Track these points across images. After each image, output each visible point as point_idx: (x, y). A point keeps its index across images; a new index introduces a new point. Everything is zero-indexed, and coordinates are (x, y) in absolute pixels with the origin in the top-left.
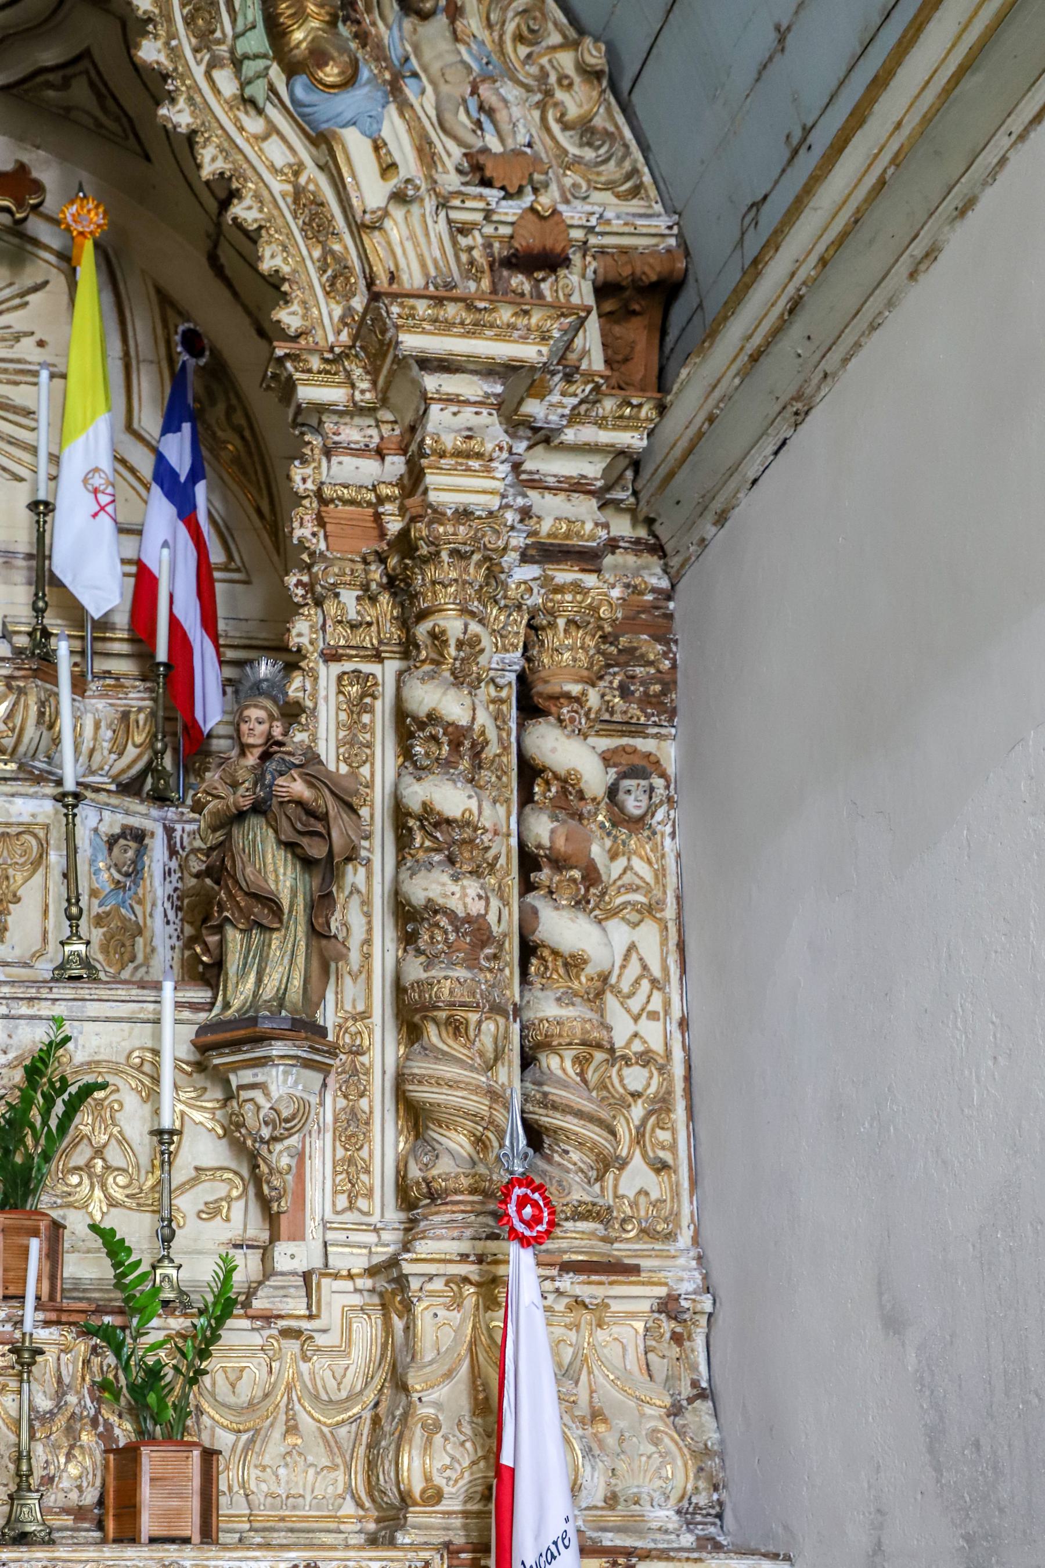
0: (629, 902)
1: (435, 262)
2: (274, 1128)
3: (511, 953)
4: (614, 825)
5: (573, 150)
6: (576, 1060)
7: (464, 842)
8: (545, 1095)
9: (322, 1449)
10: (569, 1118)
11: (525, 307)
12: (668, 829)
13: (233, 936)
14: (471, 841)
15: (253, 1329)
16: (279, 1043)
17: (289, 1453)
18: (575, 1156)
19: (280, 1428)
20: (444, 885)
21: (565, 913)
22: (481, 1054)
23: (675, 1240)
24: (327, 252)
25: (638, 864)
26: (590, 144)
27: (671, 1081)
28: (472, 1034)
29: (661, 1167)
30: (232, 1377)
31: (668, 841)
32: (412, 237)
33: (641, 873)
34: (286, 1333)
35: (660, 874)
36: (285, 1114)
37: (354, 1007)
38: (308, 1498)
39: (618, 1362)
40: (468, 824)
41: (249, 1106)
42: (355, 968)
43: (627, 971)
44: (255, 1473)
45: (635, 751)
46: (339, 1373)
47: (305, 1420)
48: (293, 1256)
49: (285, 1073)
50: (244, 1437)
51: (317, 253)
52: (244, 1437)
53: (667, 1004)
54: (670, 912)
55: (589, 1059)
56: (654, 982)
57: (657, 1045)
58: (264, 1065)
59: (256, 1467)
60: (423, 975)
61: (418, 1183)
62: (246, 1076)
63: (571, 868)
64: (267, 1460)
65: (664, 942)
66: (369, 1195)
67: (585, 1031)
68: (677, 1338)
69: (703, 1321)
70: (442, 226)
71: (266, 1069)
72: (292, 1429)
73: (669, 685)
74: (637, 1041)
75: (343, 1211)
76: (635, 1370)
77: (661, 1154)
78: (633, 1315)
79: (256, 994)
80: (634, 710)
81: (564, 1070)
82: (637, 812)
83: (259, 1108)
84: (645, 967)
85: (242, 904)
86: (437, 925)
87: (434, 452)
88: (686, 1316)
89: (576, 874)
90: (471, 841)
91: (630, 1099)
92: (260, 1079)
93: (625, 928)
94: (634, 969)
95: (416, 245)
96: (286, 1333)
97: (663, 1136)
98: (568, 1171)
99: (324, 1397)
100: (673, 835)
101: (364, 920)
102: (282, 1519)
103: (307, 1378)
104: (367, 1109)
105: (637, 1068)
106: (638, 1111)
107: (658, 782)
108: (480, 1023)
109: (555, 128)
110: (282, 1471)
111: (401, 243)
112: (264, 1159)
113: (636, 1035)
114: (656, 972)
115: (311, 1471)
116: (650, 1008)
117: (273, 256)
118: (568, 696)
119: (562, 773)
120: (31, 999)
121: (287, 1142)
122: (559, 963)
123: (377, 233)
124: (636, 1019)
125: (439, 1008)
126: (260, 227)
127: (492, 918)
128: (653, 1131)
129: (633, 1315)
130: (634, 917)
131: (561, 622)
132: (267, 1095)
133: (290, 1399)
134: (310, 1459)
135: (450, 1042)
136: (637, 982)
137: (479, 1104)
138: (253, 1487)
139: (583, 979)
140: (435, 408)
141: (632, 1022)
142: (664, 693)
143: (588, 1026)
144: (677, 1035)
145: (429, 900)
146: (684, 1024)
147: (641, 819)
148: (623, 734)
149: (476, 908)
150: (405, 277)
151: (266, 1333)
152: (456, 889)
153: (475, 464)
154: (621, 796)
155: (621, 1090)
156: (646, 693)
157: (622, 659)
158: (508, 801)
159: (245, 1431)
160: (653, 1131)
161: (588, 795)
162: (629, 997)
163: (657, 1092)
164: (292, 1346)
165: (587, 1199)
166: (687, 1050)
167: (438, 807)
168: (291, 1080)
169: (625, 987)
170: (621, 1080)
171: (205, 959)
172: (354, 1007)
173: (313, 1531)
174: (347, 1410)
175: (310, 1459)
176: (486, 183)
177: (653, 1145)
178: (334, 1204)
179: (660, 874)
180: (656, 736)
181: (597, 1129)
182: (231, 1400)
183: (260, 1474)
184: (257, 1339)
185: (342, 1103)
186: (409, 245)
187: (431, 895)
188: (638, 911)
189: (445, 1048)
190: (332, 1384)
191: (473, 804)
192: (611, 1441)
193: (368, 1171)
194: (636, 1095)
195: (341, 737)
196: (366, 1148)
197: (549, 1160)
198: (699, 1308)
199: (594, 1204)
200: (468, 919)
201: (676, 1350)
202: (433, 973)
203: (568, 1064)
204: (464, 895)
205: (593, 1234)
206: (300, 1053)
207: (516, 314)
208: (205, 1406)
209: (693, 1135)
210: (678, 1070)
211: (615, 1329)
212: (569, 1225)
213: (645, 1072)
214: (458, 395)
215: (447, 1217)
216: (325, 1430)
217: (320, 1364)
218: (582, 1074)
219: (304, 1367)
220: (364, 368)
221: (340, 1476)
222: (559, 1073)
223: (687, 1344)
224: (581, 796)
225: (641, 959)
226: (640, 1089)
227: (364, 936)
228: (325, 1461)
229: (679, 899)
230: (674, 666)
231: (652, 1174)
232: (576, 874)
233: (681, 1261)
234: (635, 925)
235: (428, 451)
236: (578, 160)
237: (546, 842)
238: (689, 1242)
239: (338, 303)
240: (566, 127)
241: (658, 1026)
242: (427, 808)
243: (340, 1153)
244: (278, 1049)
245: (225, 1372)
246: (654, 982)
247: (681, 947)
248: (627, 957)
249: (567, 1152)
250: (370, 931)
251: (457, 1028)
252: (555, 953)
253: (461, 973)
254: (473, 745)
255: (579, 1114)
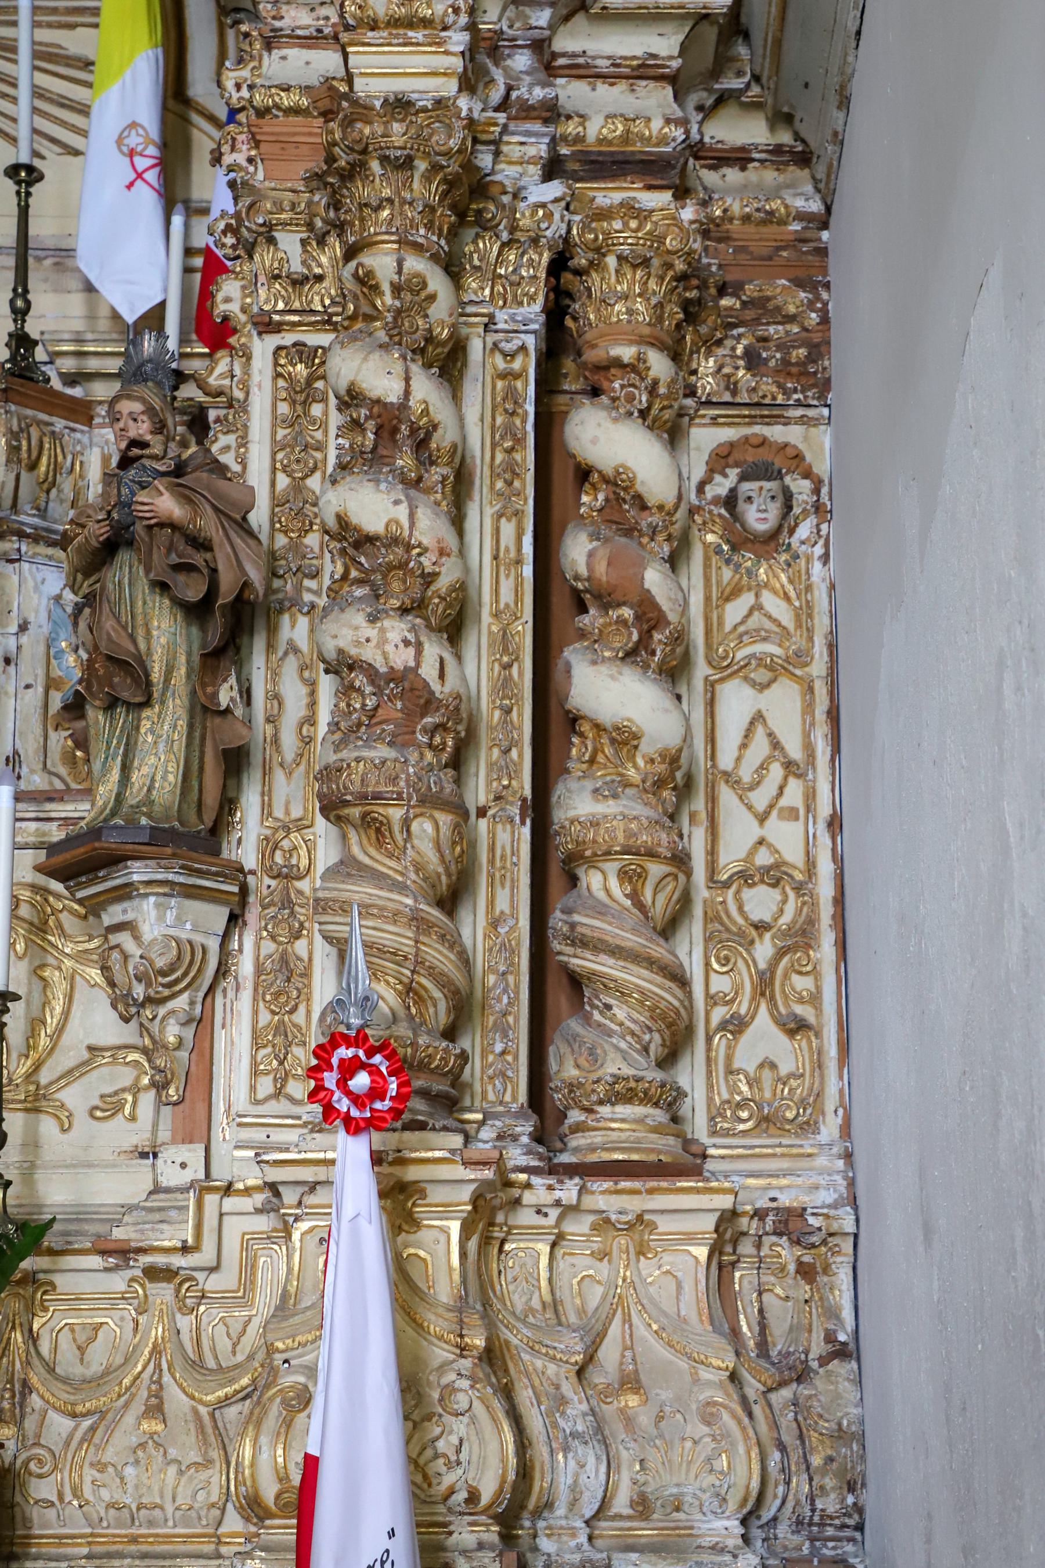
0: (753, 656)
2: (149, 985)
3: (520, 728)
4: (734, 548)
6: (623, 875)
7: (391, 567)
8: (573, 926)
10: (603, 958)
12: (819, 550)
14: (403, 565)
15: (107, 1270)
17: (142, 1445)
18: (620, 1012)
19: (138, 1407)
20: (357, 628)
21: (604, 669)
22: (418, 868)
23: (816, 1131)
25: (771, 603)
27: (814, 905)
28: (399, 838)
29: (796, 1027)
30: (82, 1338)
31: (817, 567)
33: (775, 614)
34: (152, 1273)
35: (804, 614)
36: (160, 963)
37: (287, 812)
38: (170, 1509)
39: (669, 1307)
40: (395, 541)
42: (289, 755)
43: (749, 753)
44: (89, 1474)
45: (764, 442)
46: (236, 1328)
47: (176, 1399)
48: (183, 1166)
49: (157, 905)
50: (87, 1423)
52: (87, 1423)
53: (810, 796)
54: (818, 667)
55: (642, 875)
56: (790, 767)
57: (793, 854)
58: (129, 897)
59: (92, 1465)
63: (619, 605)
64: (109, 1455)
65: (808, 708)
67: (630, 834)
68: (806, 1272)
69: (847, 1246)
71: (136, 902)
72: (156, 1409)
73: (819, 349)
74: (763, 850)
75: (266, 1099)
76: (693, 1317)
77: (799, 1009)
78: (690, 1238)
79: (119, 798)
80: (768, 386)
81: (607, 891)
82: (761, 527)
83: (126, 957)
84: (776, 745)
88: (815, 1239)
89: (627, 613)
90: (403, 565)
91: (754, 933)
92: (129, 916)
93: (748, 691)
94: (760, 747)
96: (152, 1273)
97: (802, 983)
98: (610, 1033)
99: (211, 1364)
100: (825, 558)
101: (304, 690)
102: (134, 1540)
103: (186, 1338)
104: (305, 955)
105: (762, 889)
106: (764, 950)
107: (801, 488)
108: (406, 823)
110: (129, 1471)
113: (761, 842)
114: (795, 751)
115: (172, 1470)
116: (783, 802)
118: (617, 363)
119: (609, 472)
121: (171, 1005)
122: (605, 740)
124: (762, 818)
125: (346, 804)
127: (429, 671)
128: (786, 976)
129: (690, 1238)
130: (761, 675)
131: (611, 261)
132: (137, 938)
133: (158, 1367)
134: (173, 1453)
135: (372, 851)
136: (763, 767)
138: (87, 1492)
139: (640, 762)
141: (755, 823)
142: (811, 359)
144: (824, 840)
146: (835, 824)
147: (773, 536)
148: (752, 420)
149: (402, 658)
151: (129, 1274)
152: (372, 632)
154: (741, 505)
155: (740, 921)
156: (785, 362)
157: (749, 314)
158: (518, 514)
159: (84, 1415)
160: (786, 976)
161: (652, 501)
162: (751, 789)
163: (794, 922)
164: (163, 1293)
165: (627, 1071)
166: (838, 860)
167: (354, 520)
168: (170, 916)
169: (746, 774)
170: (741, 909)
172: (287, 812)
173: (174, 1556)
174: (232, 1381)
175: (173, 1453)
177: (786, 997)
178: (253, 1088)
179: (804, 614)
180: (803, 420)
181: (645, 973)
182: (77, 1371)
183: (98, 1475)
184: (118, 1282)
185: (269, 947)
187: (342, 643)
188: (771, 669)
189: (367, 861)
190: (224, 1344)
191: (402, 512)
192: (645, 1420)
194: (761, 927)
195: (279, 437)
196: (302, 1009)
197: (587, 1019)
198: (835, 1227)
199: (638, 1080)
200: (395, 676)
201: (804, 1290)
202: (344, 754)
203: (614, 884)
205: (640, 1121)
206: (170, 877)
208: (34, 1380)
209: (843, 980)
210: (825, 889)
211: (667, 1258)
212: (605, 1110)
213: (776, 894)
216: (203, 1410)
217: (210, 1315)
218: (635, 897)
219: (185, 1323)
222: (601, 895)
223: (821, 1279)
224: (641, 504)
225: (771, 735)
226: (767, 918)
227: (303, 712)
228: (194, 1456)
229: (832, 648)
230: (825, 320)
231: (783, 1039)
232: (627, 613)
233: (822, 1161)
234: (763, 687)
237: (583, 571)
238: (836, 1133)
241: (798, 827)
243: (264, 1018)
244: (138, 872)
245: (73, 1331)
246: (790, 767)
247: (834, 716)
248: (748, 734)
249: (608, 1007)
250: (313, 704)
252: (598, 727)
253: (382, 752)
254: (414, 430)
255: (616, 952)
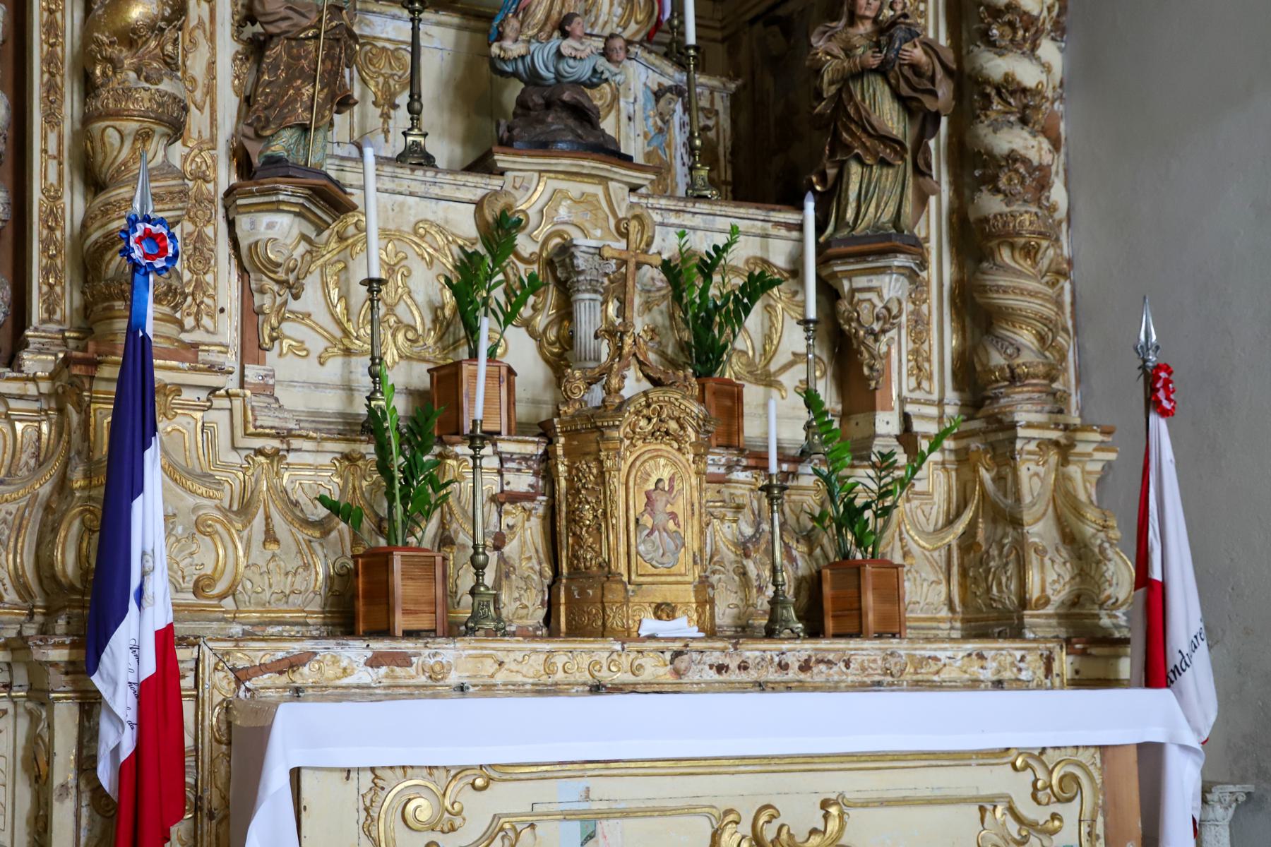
2: (885, 323)
9: (928, 568)
13: (855, 170)
16: (902, 256)
20: (1026, 139)
41: (866, 305)
60: (1006, 209)
61: (1002, 369)
62: (861, 282)
66: (930, 378)
71: (881, 277)
83: (874, 306)
85: (868, 144)
86: (1016, 171)
112: (868, 348)
120: (678, 211)
132: (881, 297)
135: (1022, 262)
137: (1048, 311)
143: (1060, 259)
145: (1013, 151)
171: (818, 188)
187: (1015, 147)
189: (1017, 266)
193: (928, 360)
196: (927, 343)
202: (1015, 208)
204: (1040, 149)
215: (1027, 396)
221: (943, 588)
242: (1008, 78)
251: (1030, 252)
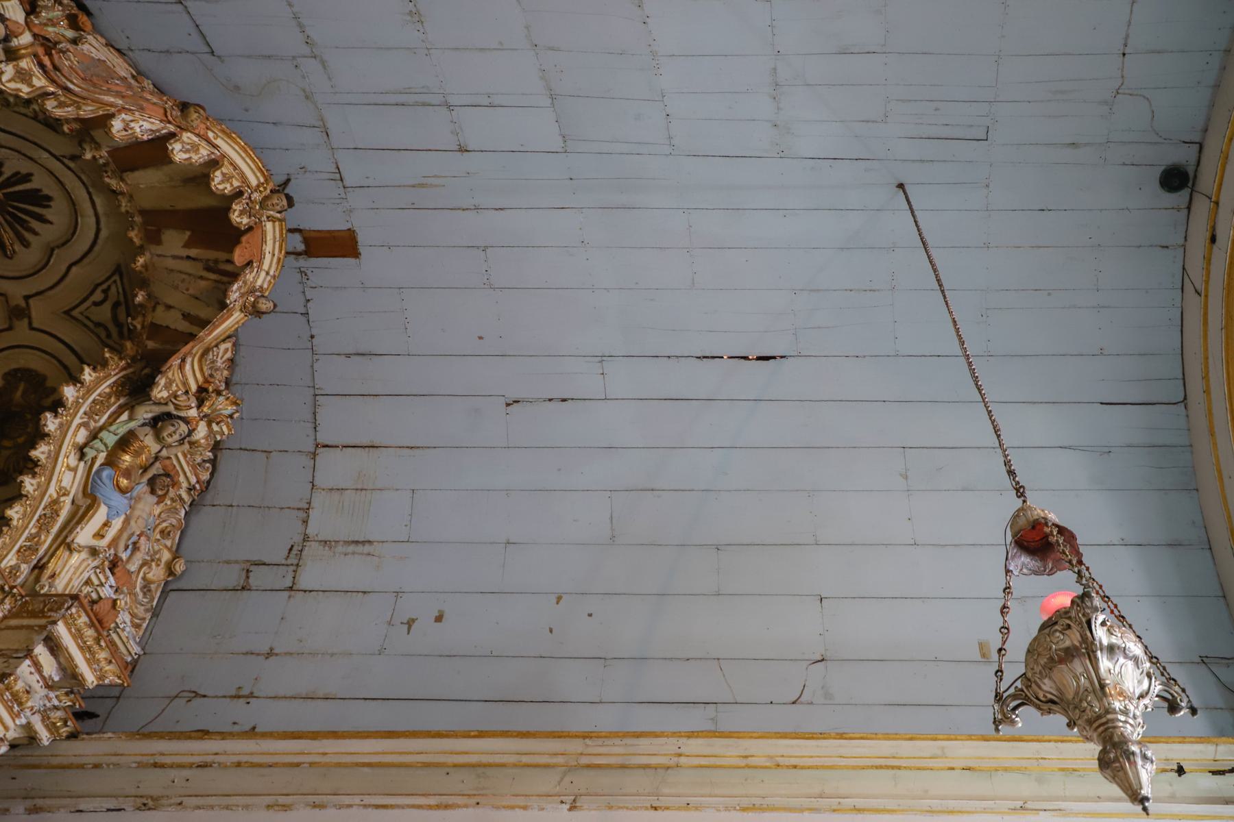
1: (73, 587)
5: (138, 589)
11: (113, 661)
24: (38, 534)
26: (145, 594)
32: (77, 568)
51: (34, 531)
70: (86, 575)
87: (9, 684)
95: (74, 573)
109: (141, 574)
111: (71, 566)
117: (17, 512)
123: (68, 553)
126: (26, 496)
140: (28, 662)
150: (57, 581)
153: (16, 708)
176: (113, 574)
186: (72, 570)
207: (106, 659)
214: (41, 666)
220: (12, 608)
235: (6, 682)
236: (135, 595)
239: (18, 559)
240: (144, 578)
